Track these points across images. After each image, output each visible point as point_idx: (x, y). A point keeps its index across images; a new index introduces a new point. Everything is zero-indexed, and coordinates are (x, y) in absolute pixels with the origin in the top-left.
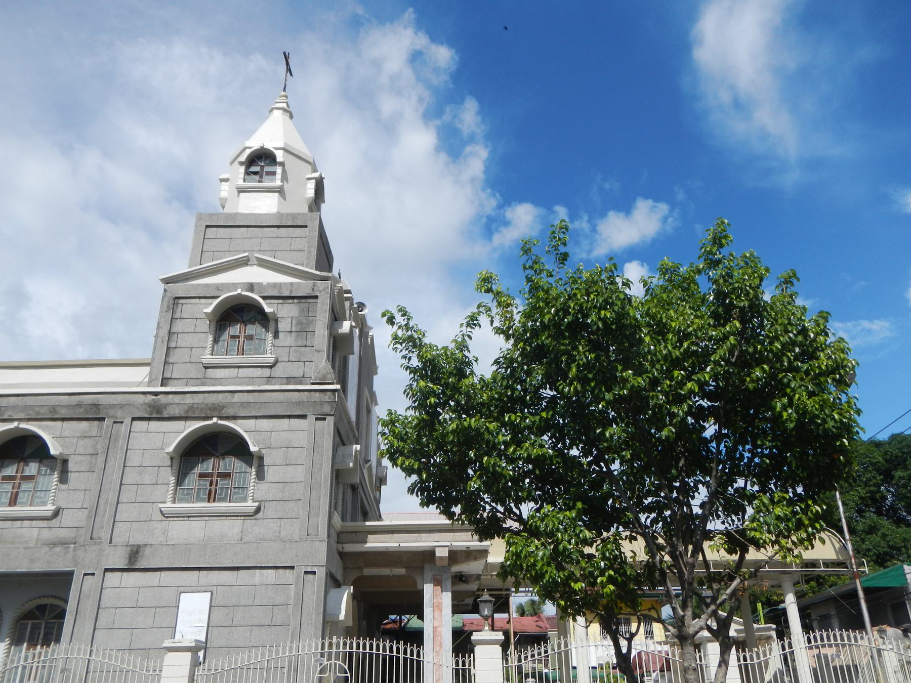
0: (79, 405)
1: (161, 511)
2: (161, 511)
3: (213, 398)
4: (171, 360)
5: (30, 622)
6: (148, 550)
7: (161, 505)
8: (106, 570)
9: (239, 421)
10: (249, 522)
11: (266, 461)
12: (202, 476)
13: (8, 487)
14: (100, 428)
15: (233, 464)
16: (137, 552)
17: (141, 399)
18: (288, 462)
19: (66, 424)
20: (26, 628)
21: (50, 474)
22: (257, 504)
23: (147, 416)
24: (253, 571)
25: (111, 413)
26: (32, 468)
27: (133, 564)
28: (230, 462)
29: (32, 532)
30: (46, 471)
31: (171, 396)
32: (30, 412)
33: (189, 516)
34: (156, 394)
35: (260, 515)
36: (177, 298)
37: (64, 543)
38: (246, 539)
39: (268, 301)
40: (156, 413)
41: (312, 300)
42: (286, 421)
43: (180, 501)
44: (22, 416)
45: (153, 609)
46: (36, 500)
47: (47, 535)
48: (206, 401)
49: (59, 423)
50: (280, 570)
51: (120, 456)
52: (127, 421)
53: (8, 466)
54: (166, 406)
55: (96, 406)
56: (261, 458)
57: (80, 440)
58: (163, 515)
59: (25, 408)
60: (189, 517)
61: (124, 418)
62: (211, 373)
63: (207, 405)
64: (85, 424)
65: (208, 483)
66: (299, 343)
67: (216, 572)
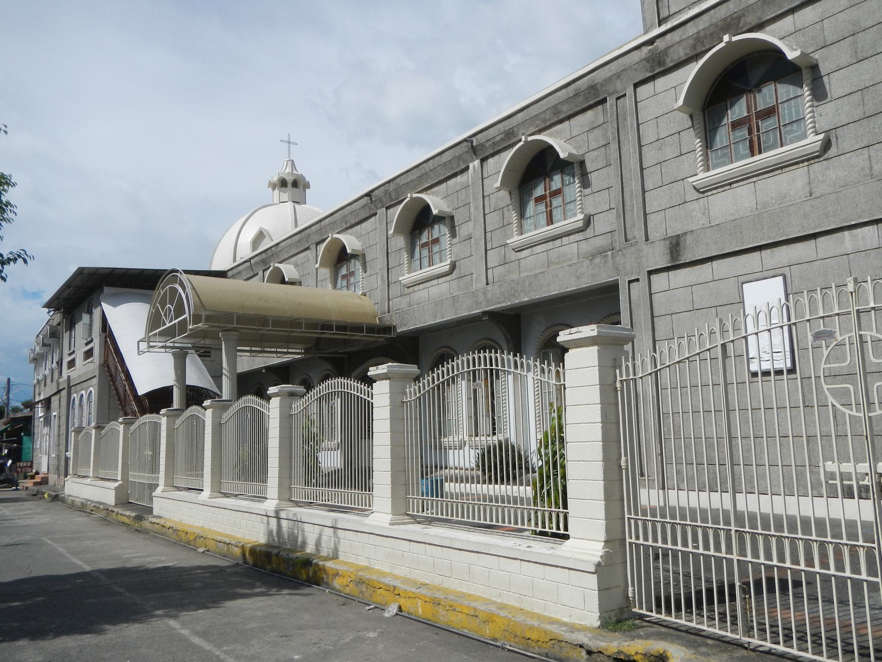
0: (576, 95)
1: (695, 188)
2: (695, 188)
6: (689, 239)
7: (691, 180)
8: (650, 273)
9: (768, 29)
10: (817, 167)
11: (824, 69)
12: (736, 125)
13: (542, 207)
14: (605, 112)
16: (678, 244)
17: (636, 56)
18: (860, 56)
19: (574, 121)
22: (821, 136)
23: (649, 75)
24: (839, 234)
25: (610, 88)
26: (557, 181)
29: (570, 248)
30: (569, 180)
31: (668, 36)
32: (538, 122)
33: (729, 183)
34: (651, 42)
35: (832, 151)
37: (601, 252)
40: (658, 66)
43: (716, 166)
44: (533, 129)
45: (714, 310)
46: (569, 214)
47: (585, 247)
49: (567, 123)
51: (632, 136)
52: (630, 91)
54: (666, 51)
55: (593, 88)
56: (814, 68)
57: (590, 134)
58: (698, 190)
59: (533, 119)
60: (730, 184)
61: (625, 89)
63: (716, 25)
64: (590, 114)
65: (746, 132)
67: (783, 249)
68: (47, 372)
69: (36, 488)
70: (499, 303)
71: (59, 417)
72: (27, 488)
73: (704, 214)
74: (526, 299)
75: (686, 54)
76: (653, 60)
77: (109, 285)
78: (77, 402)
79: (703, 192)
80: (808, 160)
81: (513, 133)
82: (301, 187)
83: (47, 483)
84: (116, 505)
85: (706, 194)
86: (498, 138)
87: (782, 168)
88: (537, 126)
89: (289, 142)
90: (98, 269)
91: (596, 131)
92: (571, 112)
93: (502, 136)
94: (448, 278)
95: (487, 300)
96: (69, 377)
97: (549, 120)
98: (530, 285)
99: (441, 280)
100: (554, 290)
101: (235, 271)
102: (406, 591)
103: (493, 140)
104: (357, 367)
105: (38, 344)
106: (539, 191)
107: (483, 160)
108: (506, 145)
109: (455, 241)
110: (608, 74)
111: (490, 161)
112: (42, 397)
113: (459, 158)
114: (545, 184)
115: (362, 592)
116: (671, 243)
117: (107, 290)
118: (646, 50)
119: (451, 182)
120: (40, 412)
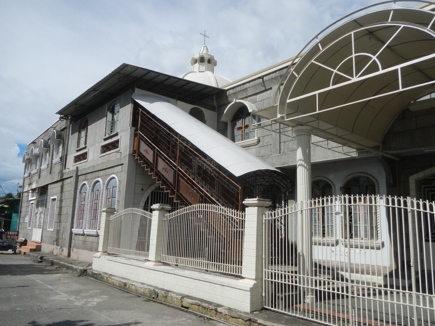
68: (44, 166)
69: (35, 254)
71: (61, 201)
72: (25, 253)
77: (139, 87)
78: (88, 188)
82: (213, 64)
83: (40, 250)
84: (252, 312)
89: (205, 36)
90: (137, 68)
96: (77, 168)
101: (231, 91)
104: (417, 172)
105: (35, 148)
112: (34, 186)
117: (137, 91)
120: (33, 198)
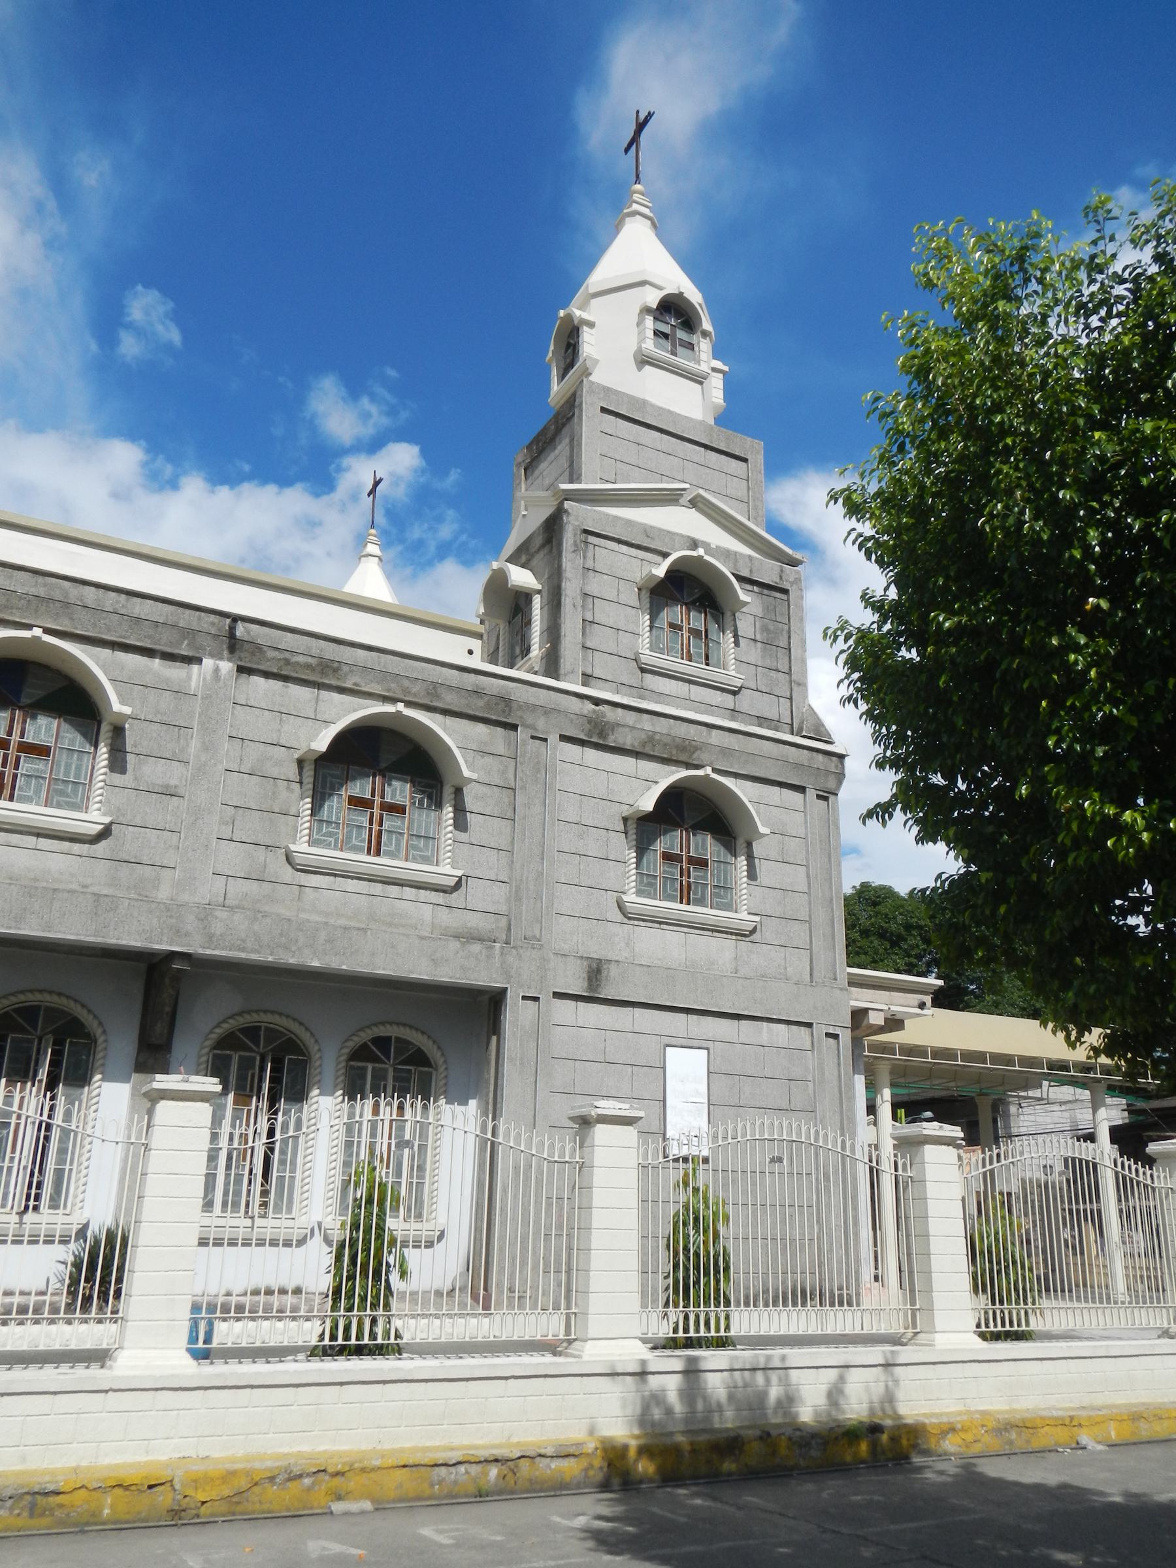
0: (477, 693)
3: (682, 730)
4: (588, 644)
5: (370, 1066)
6: (613, 971)
10: (743, 945)
15: (707, 845)
16: (598, 971)
17: (575, 705)
20: (364, 1077)
21: (429, 807)
25: (530, 720)
26: (400, 791)
27: (595, 991)
28: (704, 842)
29: (422, 910)
30: (421, 802)
31: (620, 710)
35: (754, 937)
36: (586, 532)
38: (741, 973)
39: (749, 587)
41: (778, 595)
42: (776, 789)
45: (629, 1069)
47: (446, 918)
48: (673, 732)
50: (794, 1027)
53: (354, 779)
54: (616, 725)
55: (506, 701)
60: (661, 923)
62: (651, 681)
64: (481, 728)
66: (768, 663)
70: (243, 950)
73: (627, 944)
74: (316, 963)
75: (632, 745)
76: (596, 724)
79: (630, 918)
80: (737, 934)
81: (336, 670)
85: (632, 922)
86: (301, 659)
87: (713, 931)
88: (388, 690)
91: (488, 760)
92: (456, 709)
93: (310, 660)
94: (77, 848)
95: (211, 937)
97: (415, 695)
98: (330, 941)
99: (44, 843)
100: (384, 967)
102: (1090, 1417)
103: (287, 655)
106: (361, 788)
107: (241, 670)
108: (312, 678)
109: (117, 778)
110: (532, 700)
111: (258, 680)
113: (189, 633)
114: (374, 783)
115: (1011, 1443)
116: (590, 966)
118: (590, 707)
119: (122, 656)
